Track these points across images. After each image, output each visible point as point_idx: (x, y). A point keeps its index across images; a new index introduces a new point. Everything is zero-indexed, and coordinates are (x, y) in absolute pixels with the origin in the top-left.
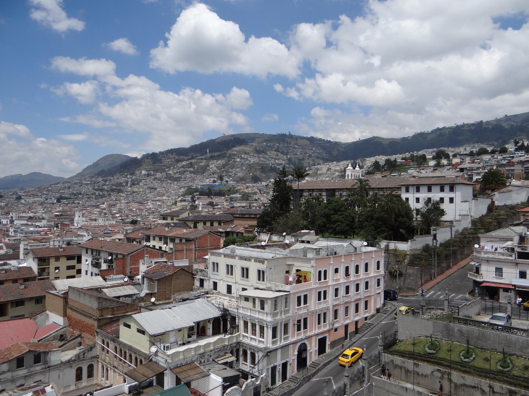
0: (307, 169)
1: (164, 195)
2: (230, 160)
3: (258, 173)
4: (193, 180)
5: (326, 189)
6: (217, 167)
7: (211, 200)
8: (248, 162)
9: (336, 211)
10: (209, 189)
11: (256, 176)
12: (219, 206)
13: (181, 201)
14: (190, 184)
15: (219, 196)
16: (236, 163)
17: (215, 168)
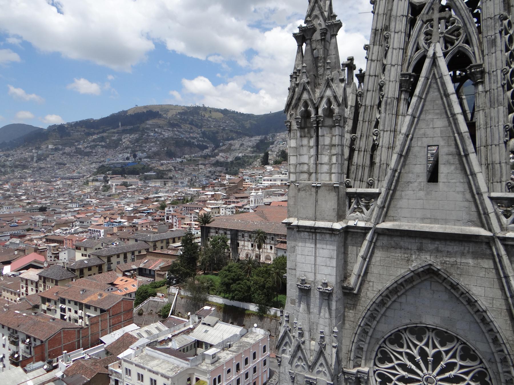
0: (221, 144)
1: (74, 171)
2: (143, 135)
3: (173, 149)
4: (105, 155)
5: (231, 230)
6: (130, 142)
7: (125, 180)
8: (162, 136)
9: (234, 280)
10: (122, 167)
11: (171, 150)
12: (133, 187)
13: (93, 180)
14: (102, 159)
15: (133, 174)
16: (150, 137)
17: (128, 143)
